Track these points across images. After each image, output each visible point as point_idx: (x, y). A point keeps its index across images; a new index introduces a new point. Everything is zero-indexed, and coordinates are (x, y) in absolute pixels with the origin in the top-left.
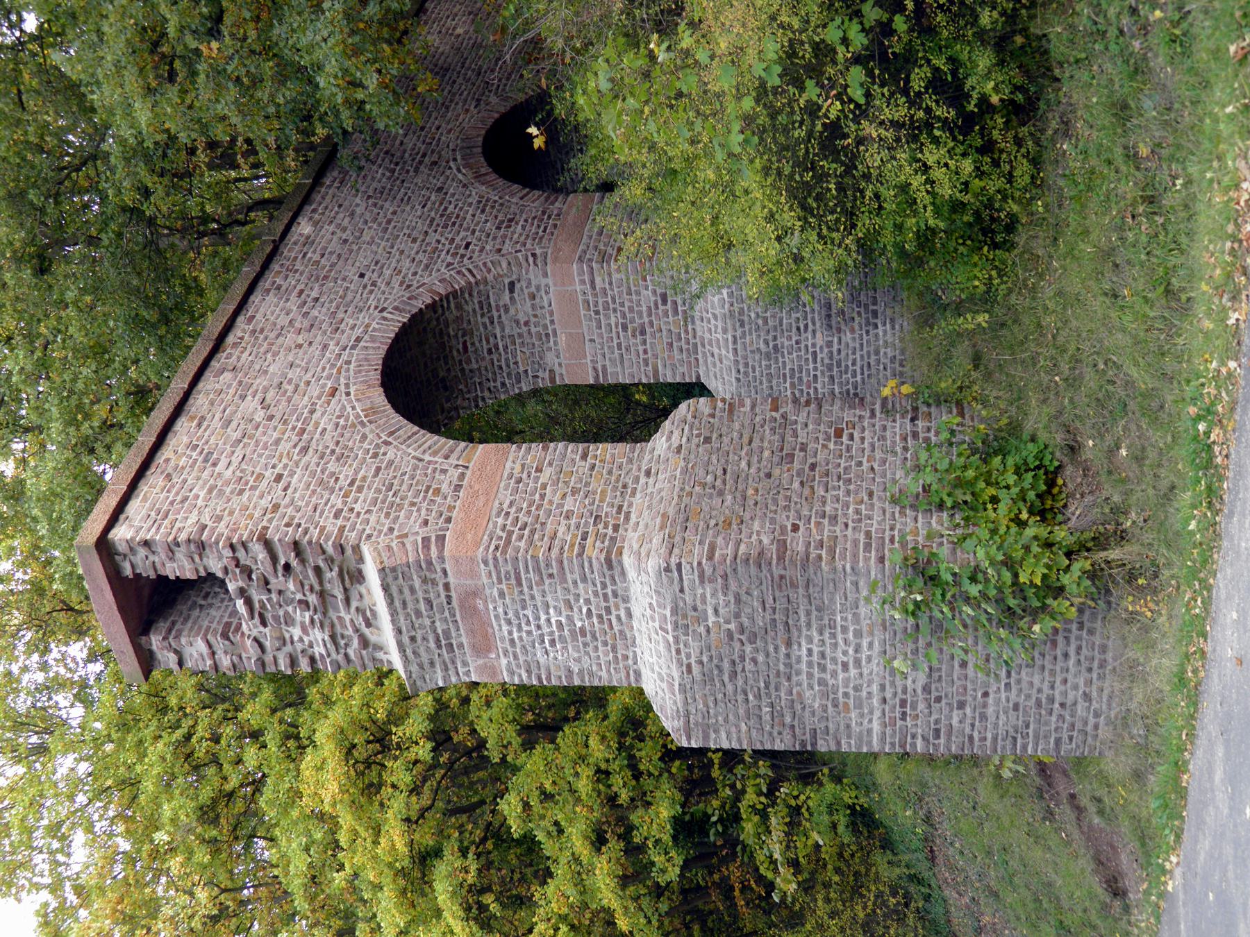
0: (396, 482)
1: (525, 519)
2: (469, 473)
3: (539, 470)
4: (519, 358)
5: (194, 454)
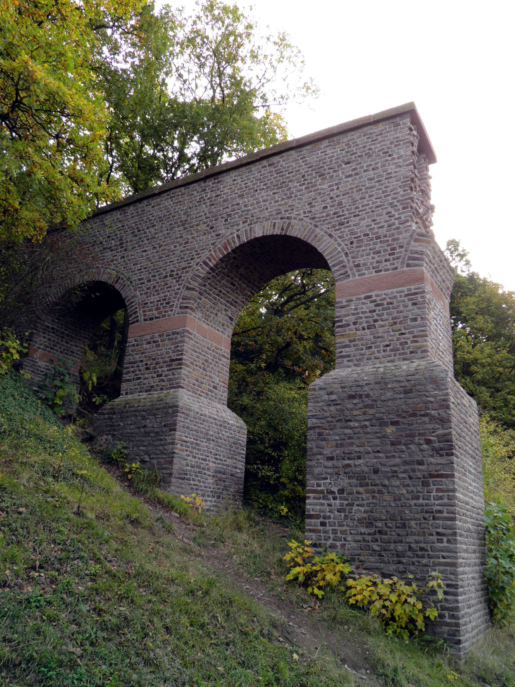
4: (207, 300)
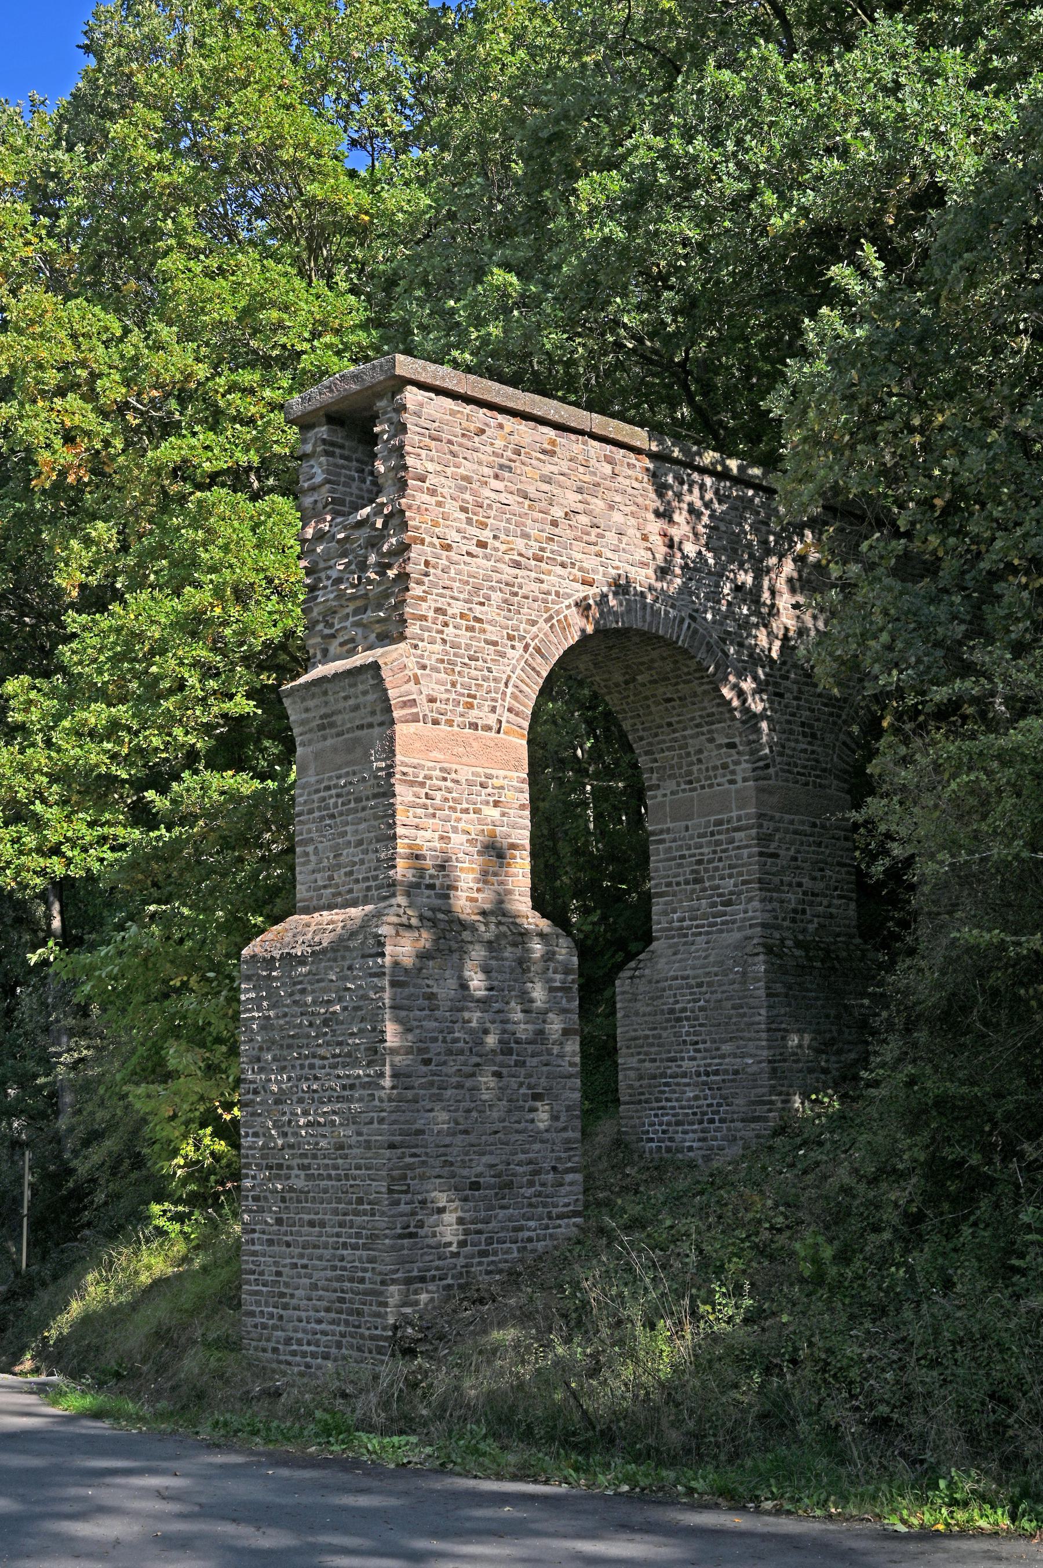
0: (480, 663)
1: (439, 798)
2: (493, 734)
3: (496, 804)
4: (667, 753)
5: (509, 454)
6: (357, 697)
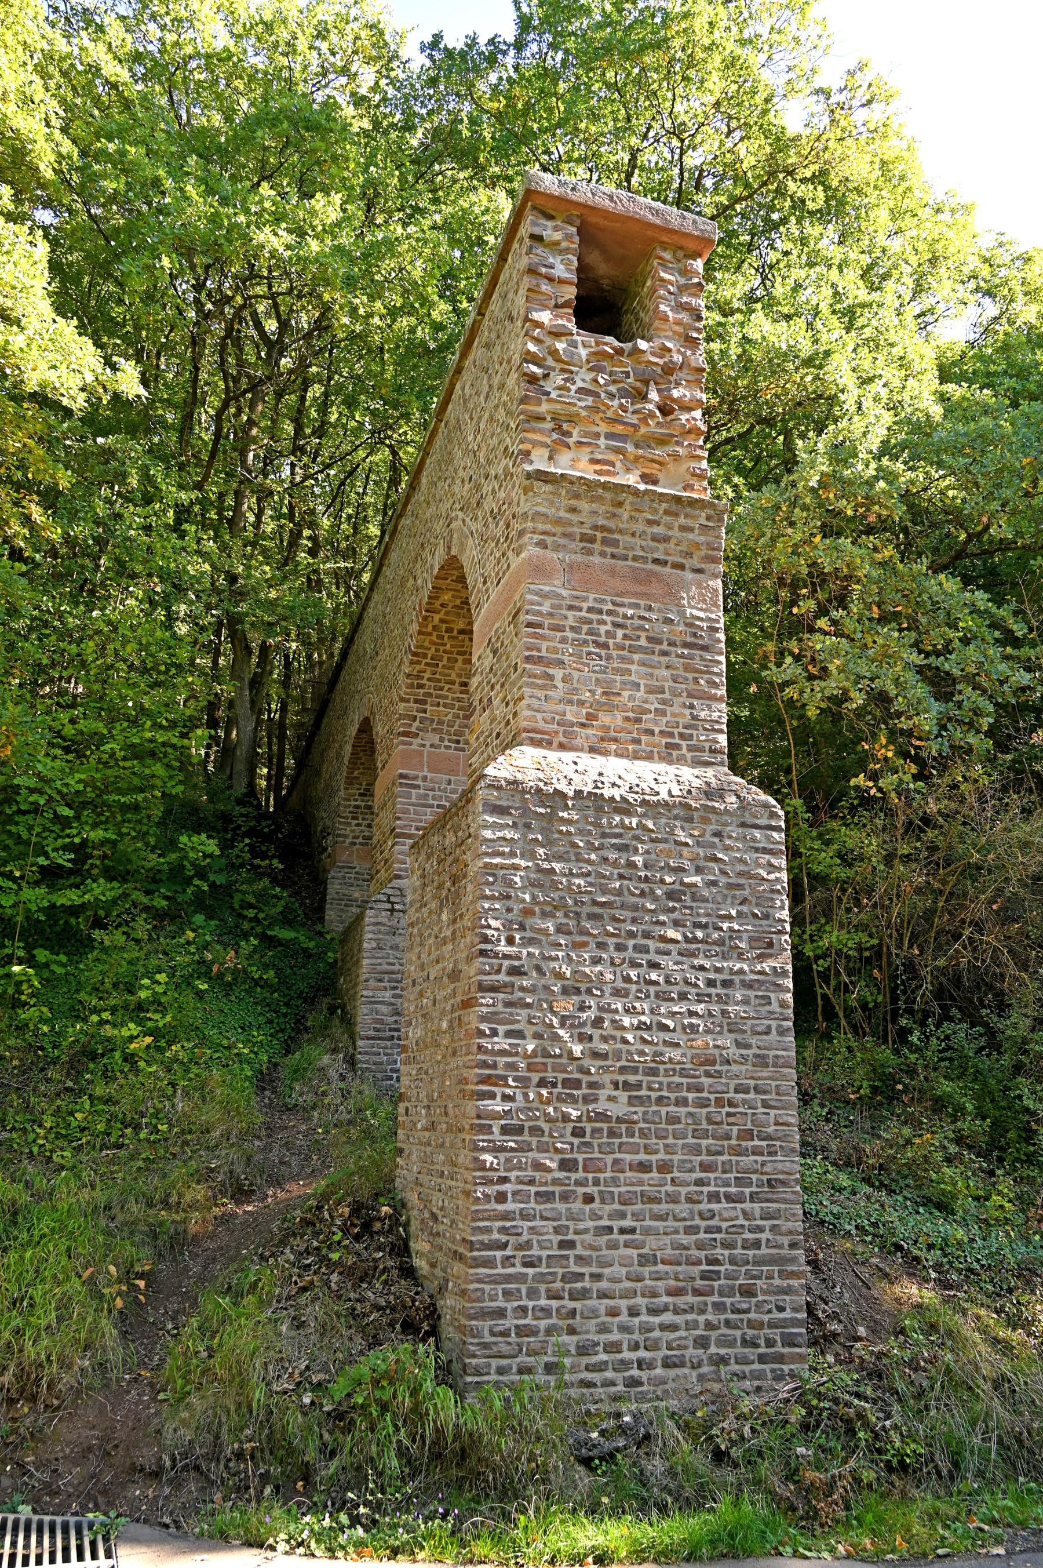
6: (670, 528)
